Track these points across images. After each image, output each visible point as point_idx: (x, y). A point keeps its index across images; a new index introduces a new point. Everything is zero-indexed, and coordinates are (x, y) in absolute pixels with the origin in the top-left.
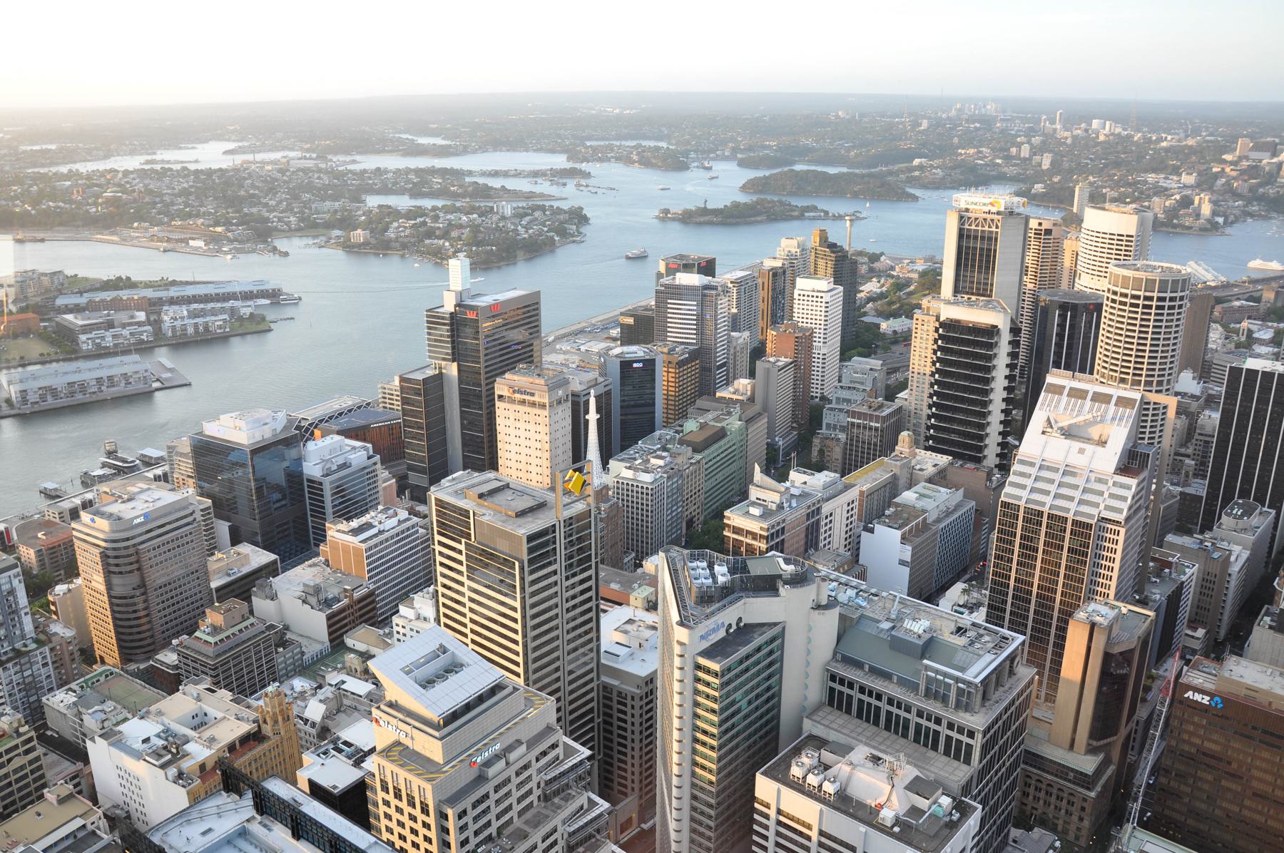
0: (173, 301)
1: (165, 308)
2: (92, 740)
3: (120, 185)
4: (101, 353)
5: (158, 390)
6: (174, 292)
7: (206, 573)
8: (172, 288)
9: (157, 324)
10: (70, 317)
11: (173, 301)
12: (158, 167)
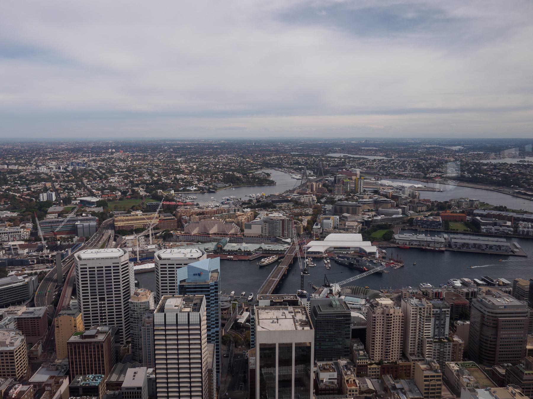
0: (524, 220)
1: (521, 222)
2: (465, 389)
3: (507, 169)
4: (489, 234)
5: (511, 255)
6: (525, 216)
7: (526, 341)
8: (525, 214)
9: (516, 227)
10: (478, 218)
11: (524, 220)
12: (526, 164)
